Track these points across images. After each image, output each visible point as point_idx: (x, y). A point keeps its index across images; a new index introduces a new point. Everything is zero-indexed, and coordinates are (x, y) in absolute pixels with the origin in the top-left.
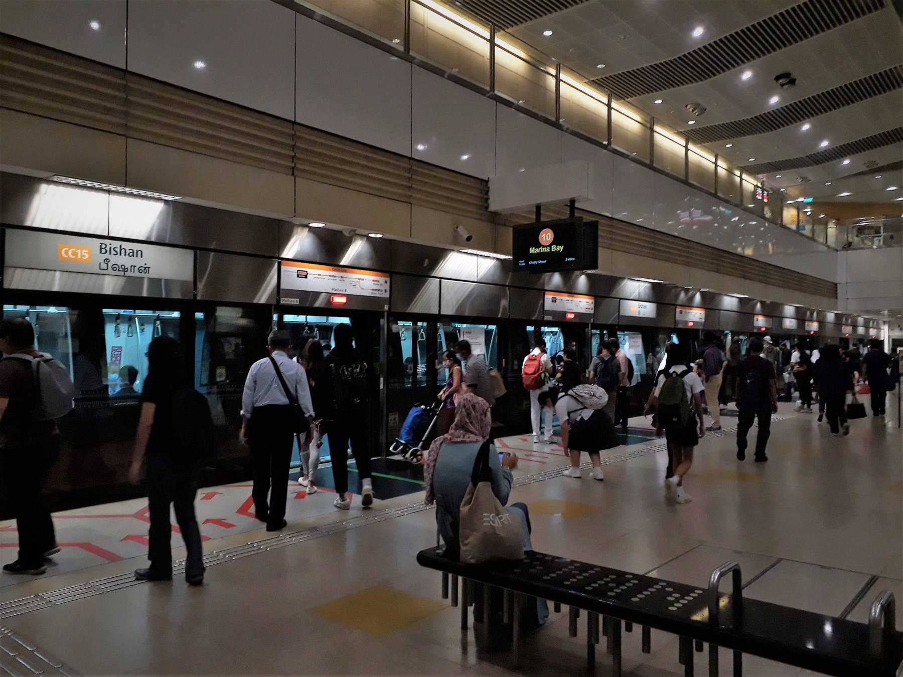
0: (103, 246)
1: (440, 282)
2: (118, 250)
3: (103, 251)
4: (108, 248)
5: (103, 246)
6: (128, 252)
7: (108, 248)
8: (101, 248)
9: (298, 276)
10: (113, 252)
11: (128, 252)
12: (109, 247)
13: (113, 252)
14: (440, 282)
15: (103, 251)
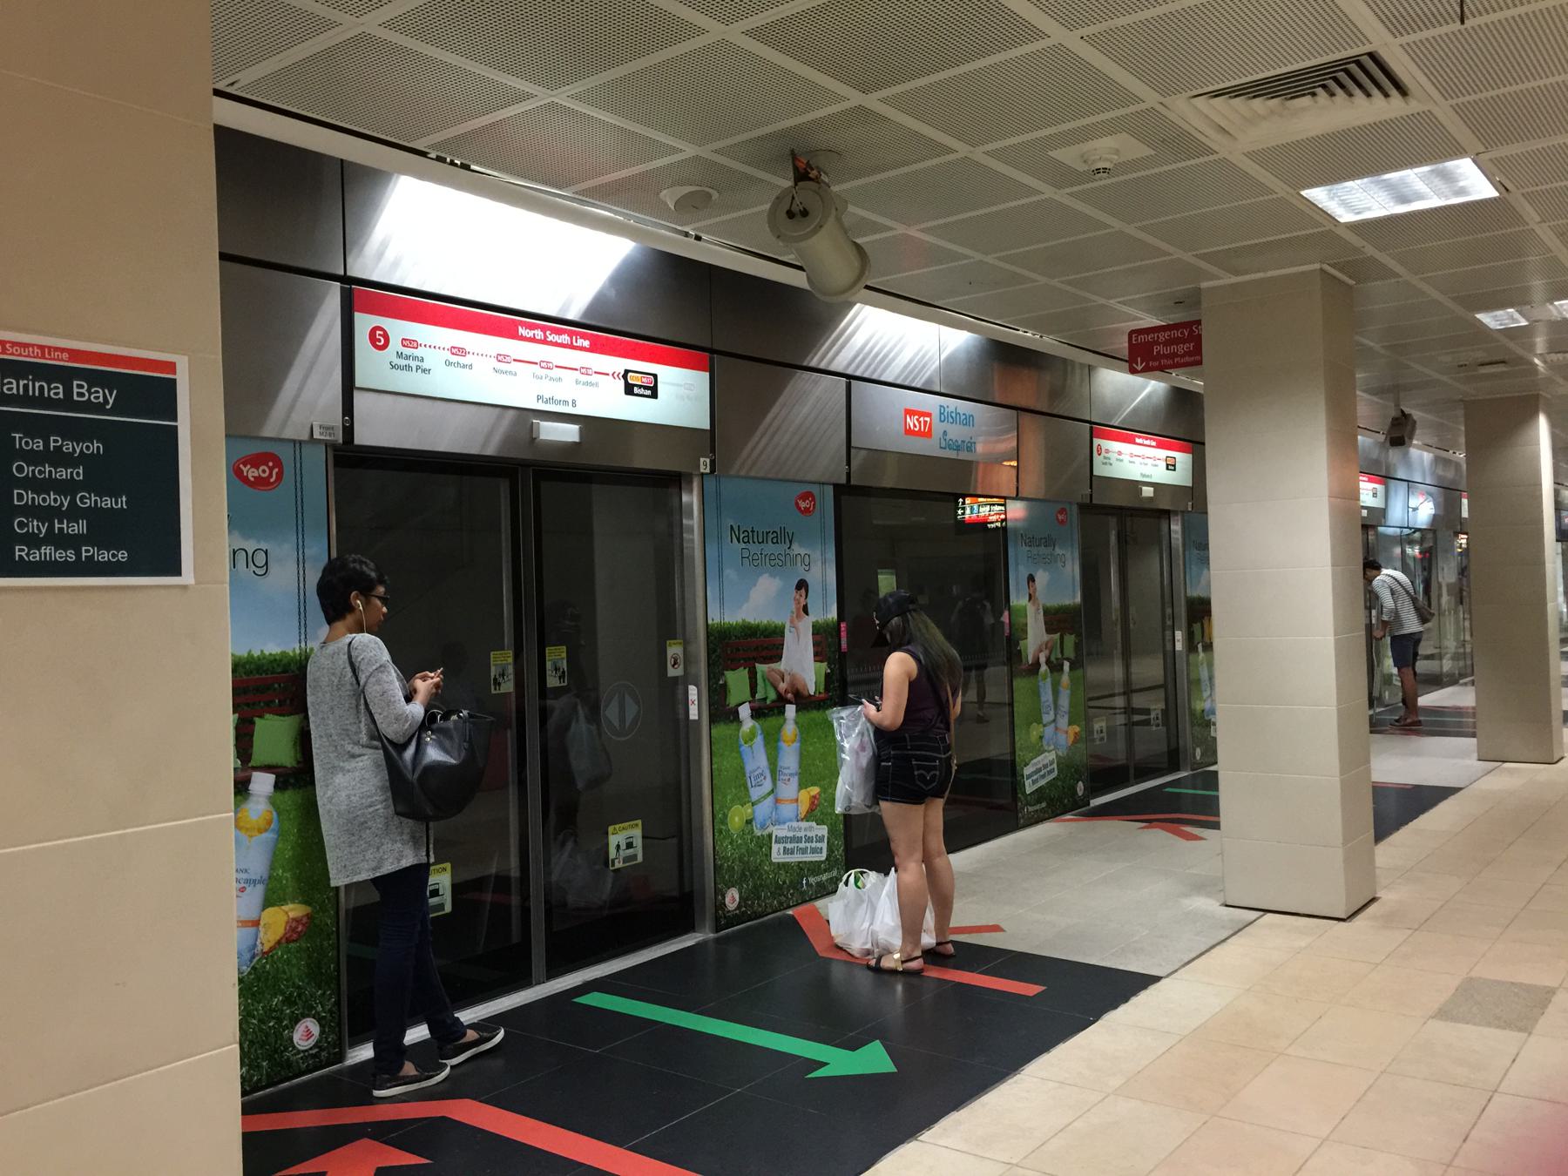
2: (954, 415)
4: (946, 414)
6: (964, 417)
7: (946, 414)
10: (951, 420)
12: (946, 410)
15: (942, 419)
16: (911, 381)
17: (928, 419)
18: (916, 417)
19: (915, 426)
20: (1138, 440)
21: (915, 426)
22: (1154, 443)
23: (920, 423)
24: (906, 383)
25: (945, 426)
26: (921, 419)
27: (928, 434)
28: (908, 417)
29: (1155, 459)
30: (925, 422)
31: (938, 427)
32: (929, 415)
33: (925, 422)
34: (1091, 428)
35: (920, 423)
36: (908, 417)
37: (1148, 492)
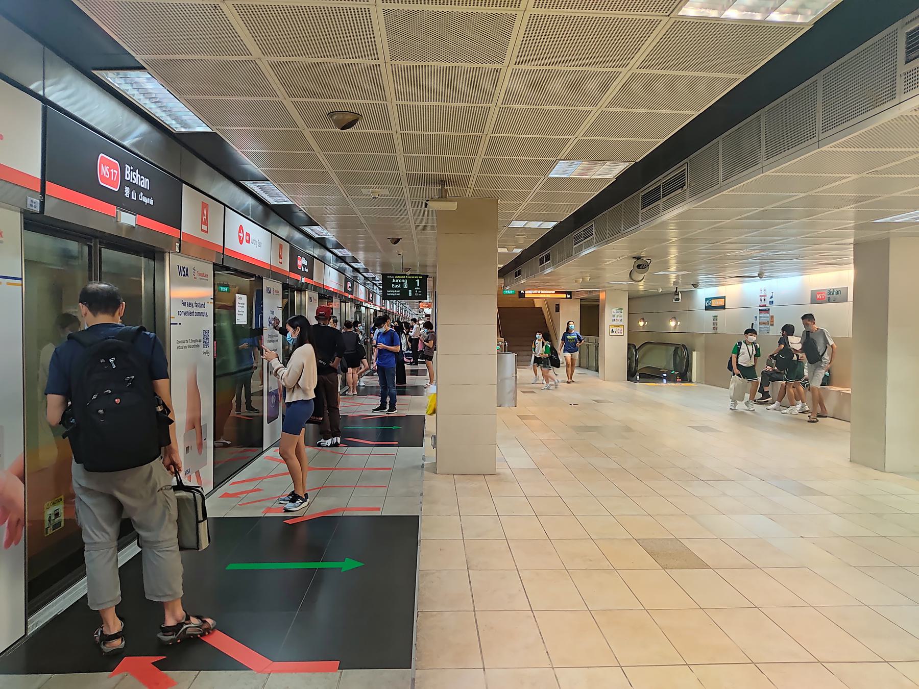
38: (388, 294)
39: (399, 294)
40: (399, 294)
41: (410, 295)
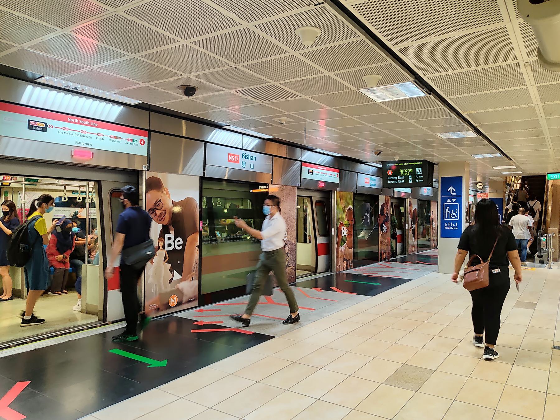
0: (243, 155)
1: (357, 174)
2: (248, 156)
3: (243, 157)
4: (245, 156)
5: (243, 155)
6: (251, 157)
7: (245, 156)
8: (243, 156)
9: (309, 174)
11: (251, 157)
12: (245, 155)
13: (246, 158)
14: (357, 174)
15: (243, 157)
16: (221, 142)
17: (238, 157)
18: (233, 156)
19: (232, 159)
20: (319, 168)
21: (232, 159)
22: (325, 169)
23: (234, 158)
24: (235, 146)
25: (244, 160)
26: (235, 157)
27: (238, 162)
28: (230, 156)
29: (326, 174)
30: (237, 158)
31: (241, 160)
32: (238, 156)
33: (237, 158)
34: (301, 163)
35: (234, 158)
36: (230, 156)
37: (323, 184)
38: (389, 182)
39: (403, 181)
40: (403, 181)
41: (410, 181)
